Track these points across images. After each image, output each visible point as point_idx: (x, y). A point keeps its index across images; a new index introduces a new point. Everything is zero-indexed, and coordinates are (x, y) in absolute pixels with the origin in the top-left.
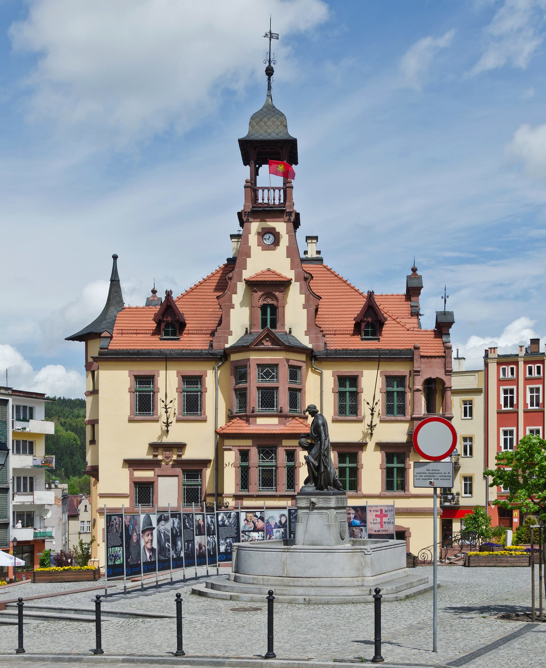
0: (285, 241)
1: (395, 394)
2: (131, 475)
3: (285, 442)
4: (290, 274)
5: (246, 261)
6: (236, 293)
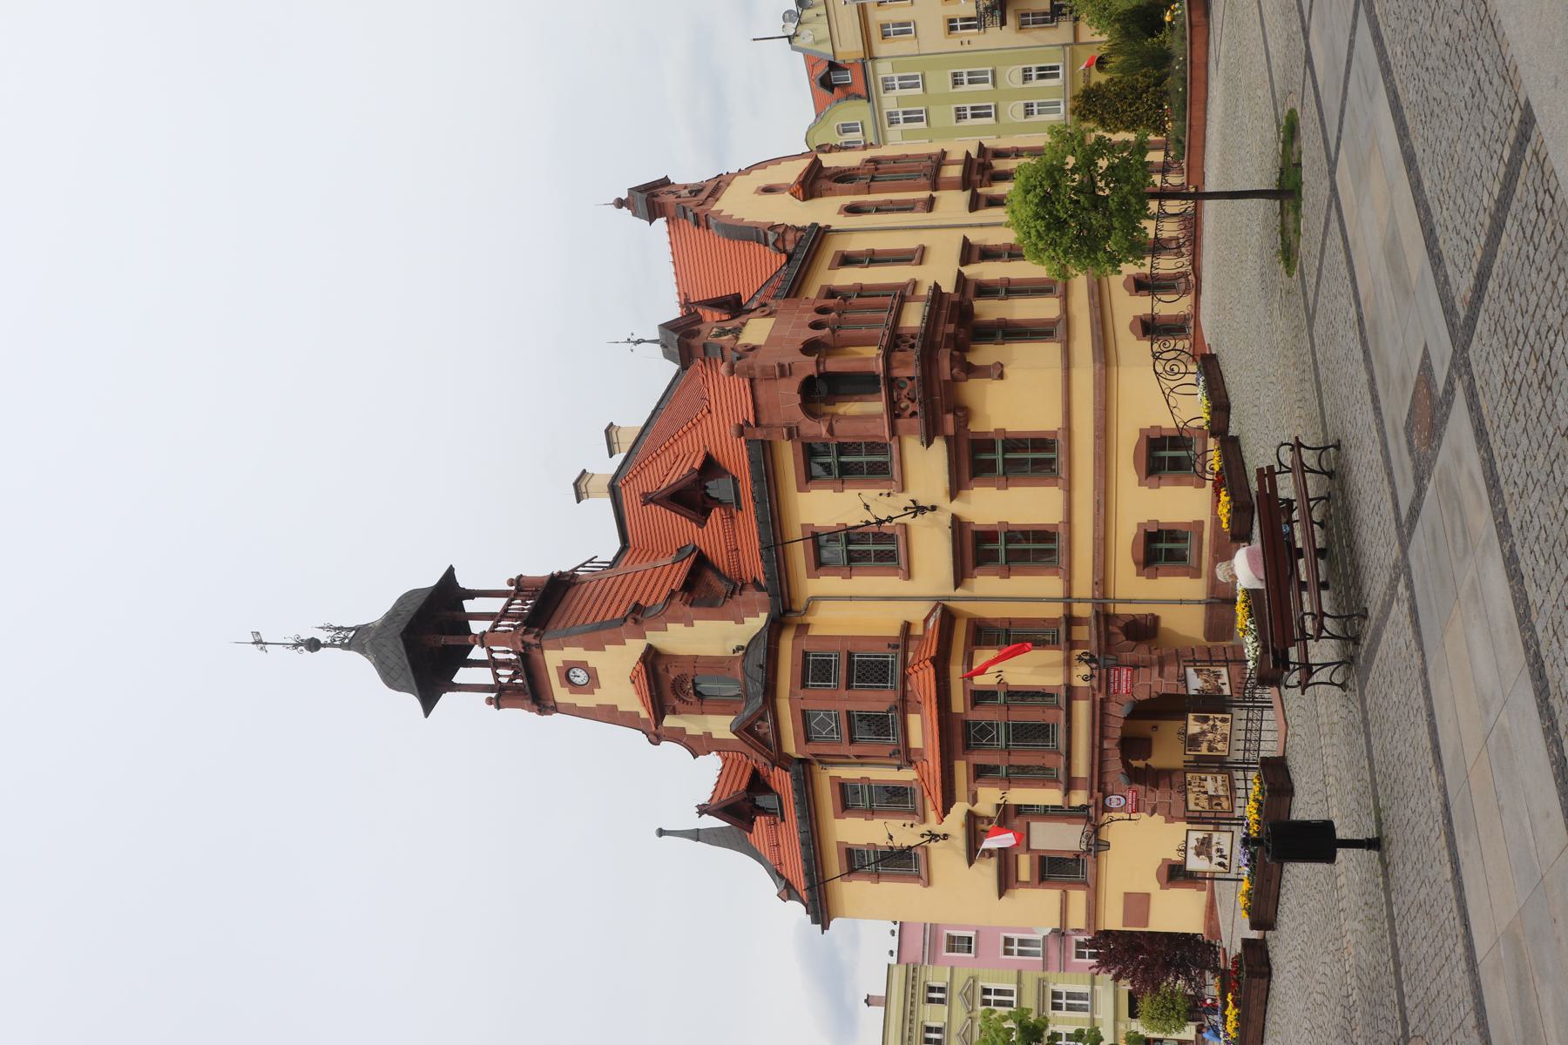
0: (573, 653)
1: (843, 459)
2: (1026, 884)
3: (958, 704)
4: (634, 649)
5: (623, 713)
6: (683, 729)
